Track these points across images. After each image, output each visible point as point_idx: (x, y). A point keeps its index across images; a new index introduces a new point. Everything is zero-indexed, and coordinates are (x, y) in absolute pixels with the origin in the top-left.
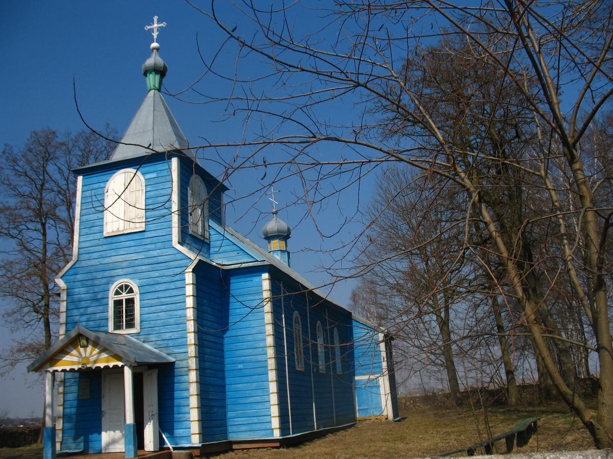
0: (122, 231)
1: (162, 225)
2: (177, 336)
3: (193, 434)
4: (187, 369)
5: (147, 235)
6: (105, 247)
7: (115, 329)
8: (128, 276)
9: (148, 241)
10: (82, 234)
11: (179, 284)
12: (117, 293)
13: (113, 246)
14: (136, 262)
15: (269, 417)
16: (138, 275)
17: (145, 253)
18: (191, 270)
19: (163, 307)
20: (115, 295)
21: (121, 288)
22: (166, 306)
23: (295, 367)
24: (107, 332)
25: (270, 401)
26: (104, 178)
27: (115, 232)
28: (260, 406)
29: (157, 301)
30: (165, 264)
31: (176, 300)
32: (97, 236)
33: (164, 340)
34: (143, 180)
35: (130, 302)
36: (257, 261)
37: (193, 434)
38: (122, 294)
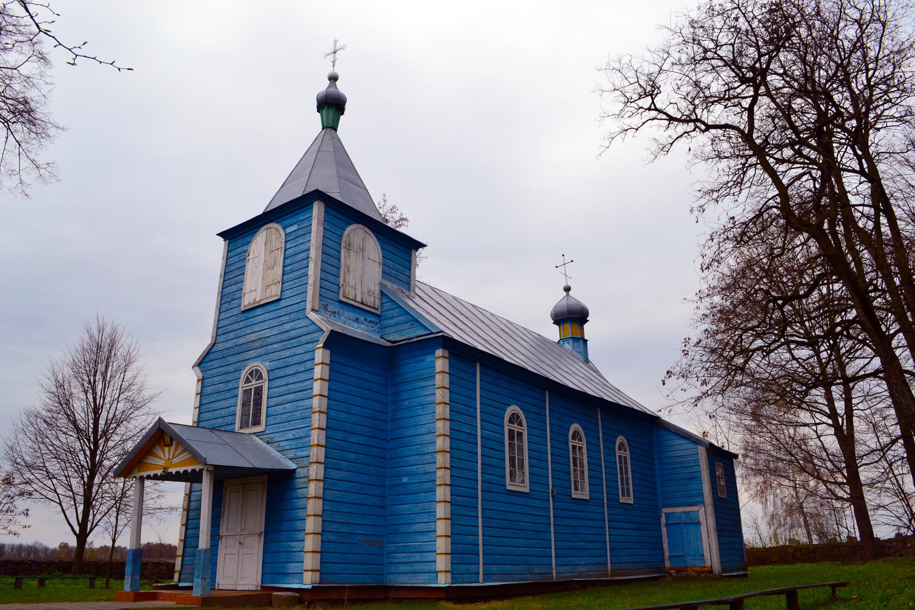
0: (259, 302)
1: (297, 290)
2: (301, 434)
3: (305, 571)
4: (306, 479)
5: (283, 304)
6: (241, 324)
7: (241, 428)
9: (282, 312)
11: (308, 365)
12: (248, 381)
13: (249, 322)
14: (269, 340)
15: (434, 554)
16: (269, 356)
18: (321, 345)
21: (251, 374)
22: (293, 395)
23: (505, 486)
24: (233, 432)
25: (436, 531)
26: (247, 239)
27: (252, 304)
28: (421, 538)
29: (284, 388)
30: (297, 340)
31: (304, 387)
32: (235, 311)
33: (287, 440)
34: (283, 236)
35: (259, 391)
36: (432, 333)
37: (305, 571)
38: (251, 382)
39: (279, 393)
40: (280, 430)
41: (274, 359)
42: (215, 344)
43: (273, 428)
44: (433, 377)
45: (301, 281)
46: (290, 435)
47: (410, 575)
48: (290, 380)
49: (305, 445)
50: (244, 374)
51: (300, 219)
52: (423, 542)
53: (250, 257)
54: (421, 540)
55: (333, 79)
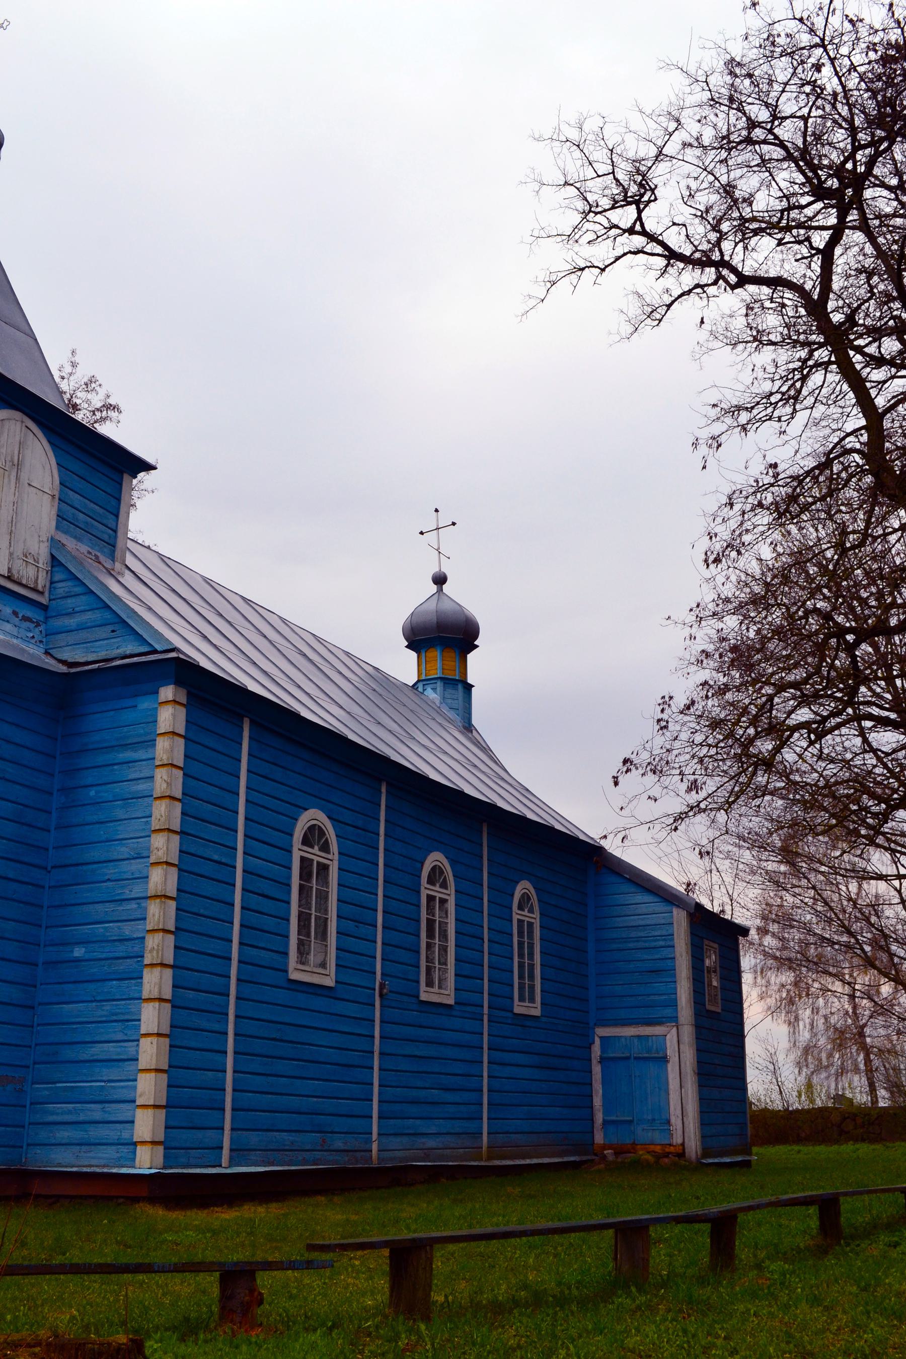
15: (132, 1105)
23: (286, 971)
25: (137, 1060)
36: (155, 652)
44: (152, 743)
54: (104, 1078)
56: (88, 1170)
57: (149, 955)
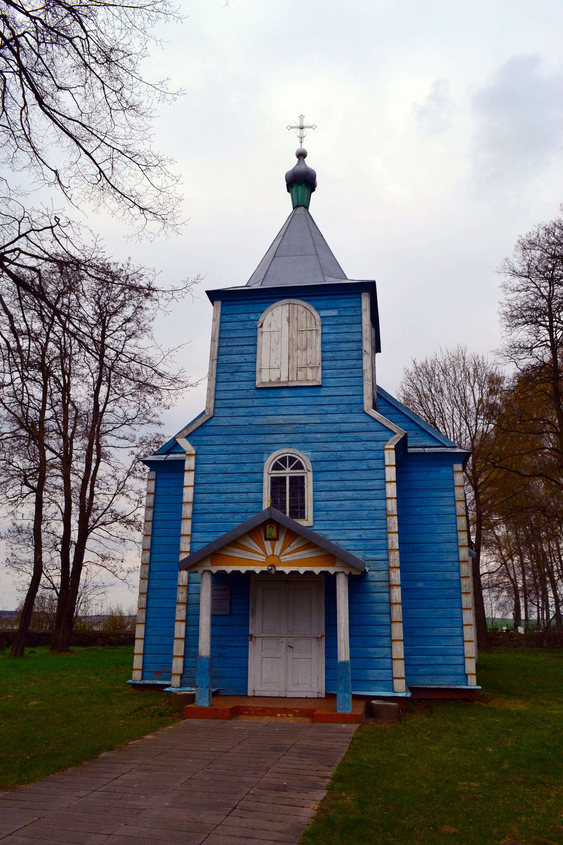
0: (285, 382)
5: (323, 392)
6: (257, 402)
8: (294, 445)
9: (326, 400)
10: (221, 380)
12: (276, 467)
13: (271, 401)
16: (310, 446)
17: (322, 417)
19: (350, 493)
20: (273, 469)
21: (283, 460)
22: (353, 493)
26: (257, 308)
29: (339, 484)
31: (371, 486)
32: (244, 385)
33: (350, 540)
36: (445, 446)
39: (331, 488)
40: (338, 528)
41: (320, 450)
42: (213, 417)
43: (326, 524)
44: (453, 490)
45: (351, 372)
46: (355, 535)
47: (432, 676)
48: (346, 476)
49: (378, 548)
50: (270, 460)
51: (341, 305)
52: (446, 646)
53: (265, 328)
54: (444, 644)
55: (302, 155)
56: (445, 687)
57: (464, 588)
